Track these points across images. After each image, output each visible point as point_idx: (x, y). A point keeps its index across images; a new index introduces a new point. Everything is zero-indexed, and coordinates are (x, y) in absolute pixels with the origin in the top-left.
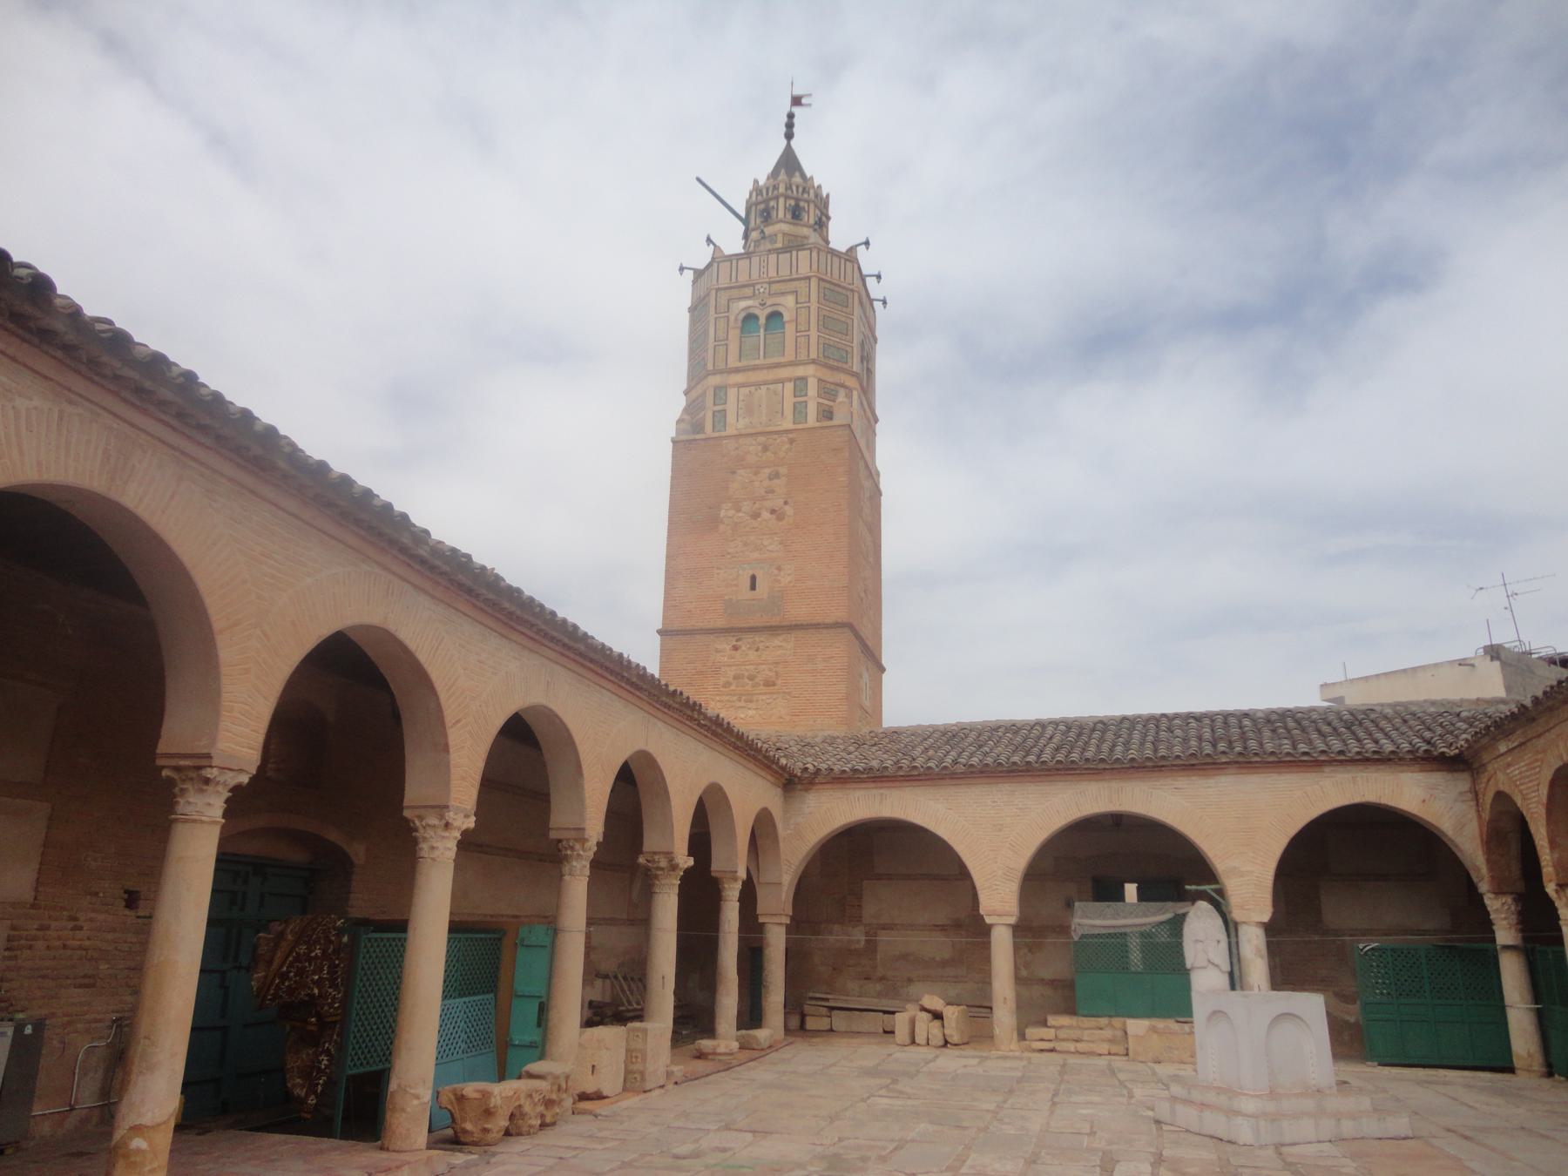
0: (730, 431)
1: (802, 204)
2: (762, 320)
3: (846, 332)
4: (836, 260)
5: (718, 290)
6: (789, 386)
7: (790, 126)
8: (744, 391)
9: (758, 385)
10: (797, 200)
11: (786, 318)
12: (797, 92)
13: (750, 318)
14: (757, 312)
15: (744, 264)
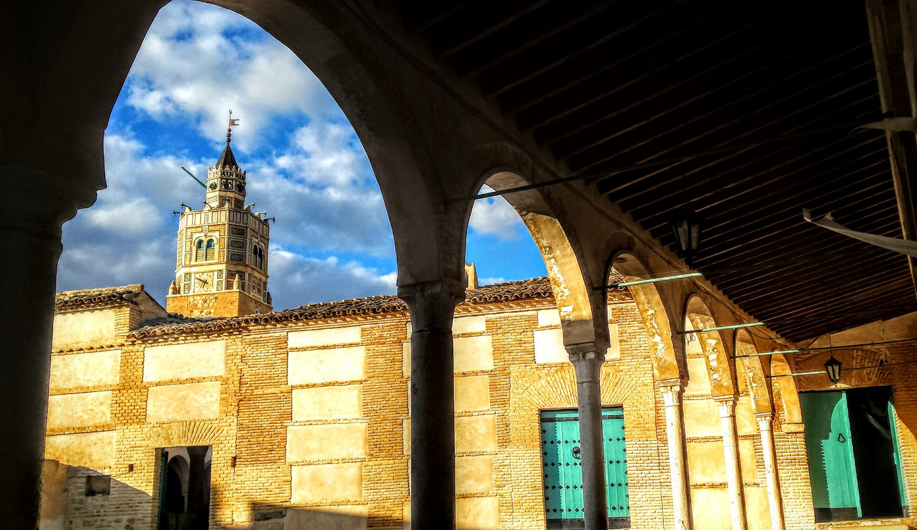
0: (191, 293)
2: (205, 244)
3: (242, 246)
6: (216, 273)
9: (203, 273)
10: (227, 180)
11: (215, 242)
13: (200, 242)
14: (203, 238)
15: (198, 216)
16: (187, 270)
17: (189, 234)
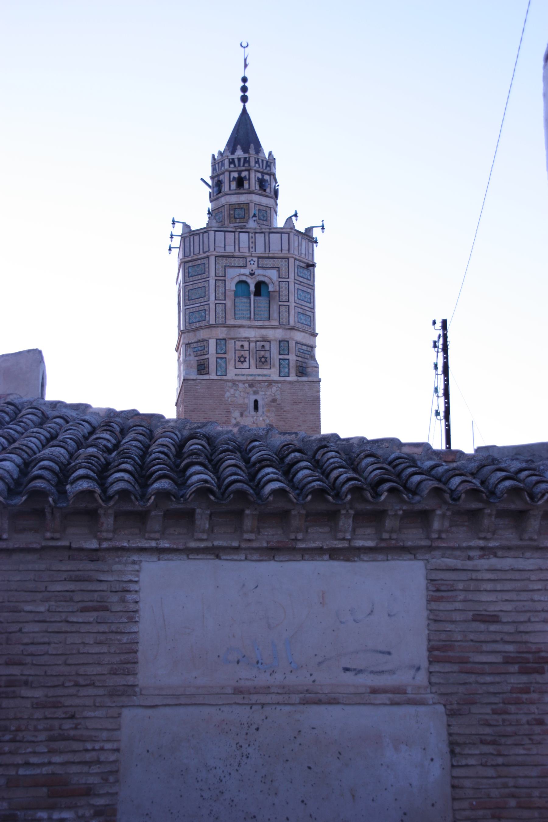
2: (252, 288)
7: (244, 89)
10: (263, 173)
11: (271, 289)
14: (249, 280)
16: (221, 333)
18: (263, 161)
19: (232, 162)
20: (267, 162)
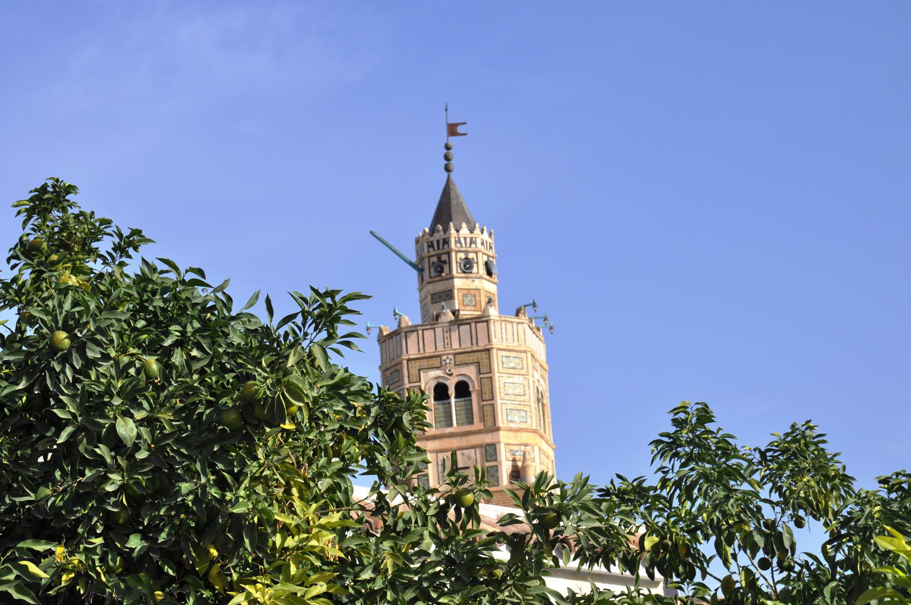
1: (471, 256)
2: (452, 391)
4: (509, 325)
5: (409, 360)
8: (441, 456)
10: (466, 252)
12: (451, 121)
15: (429, 334)
17: (414, 371)
18: (465, 239)
19: (431, 245)
20: (471, 239)
